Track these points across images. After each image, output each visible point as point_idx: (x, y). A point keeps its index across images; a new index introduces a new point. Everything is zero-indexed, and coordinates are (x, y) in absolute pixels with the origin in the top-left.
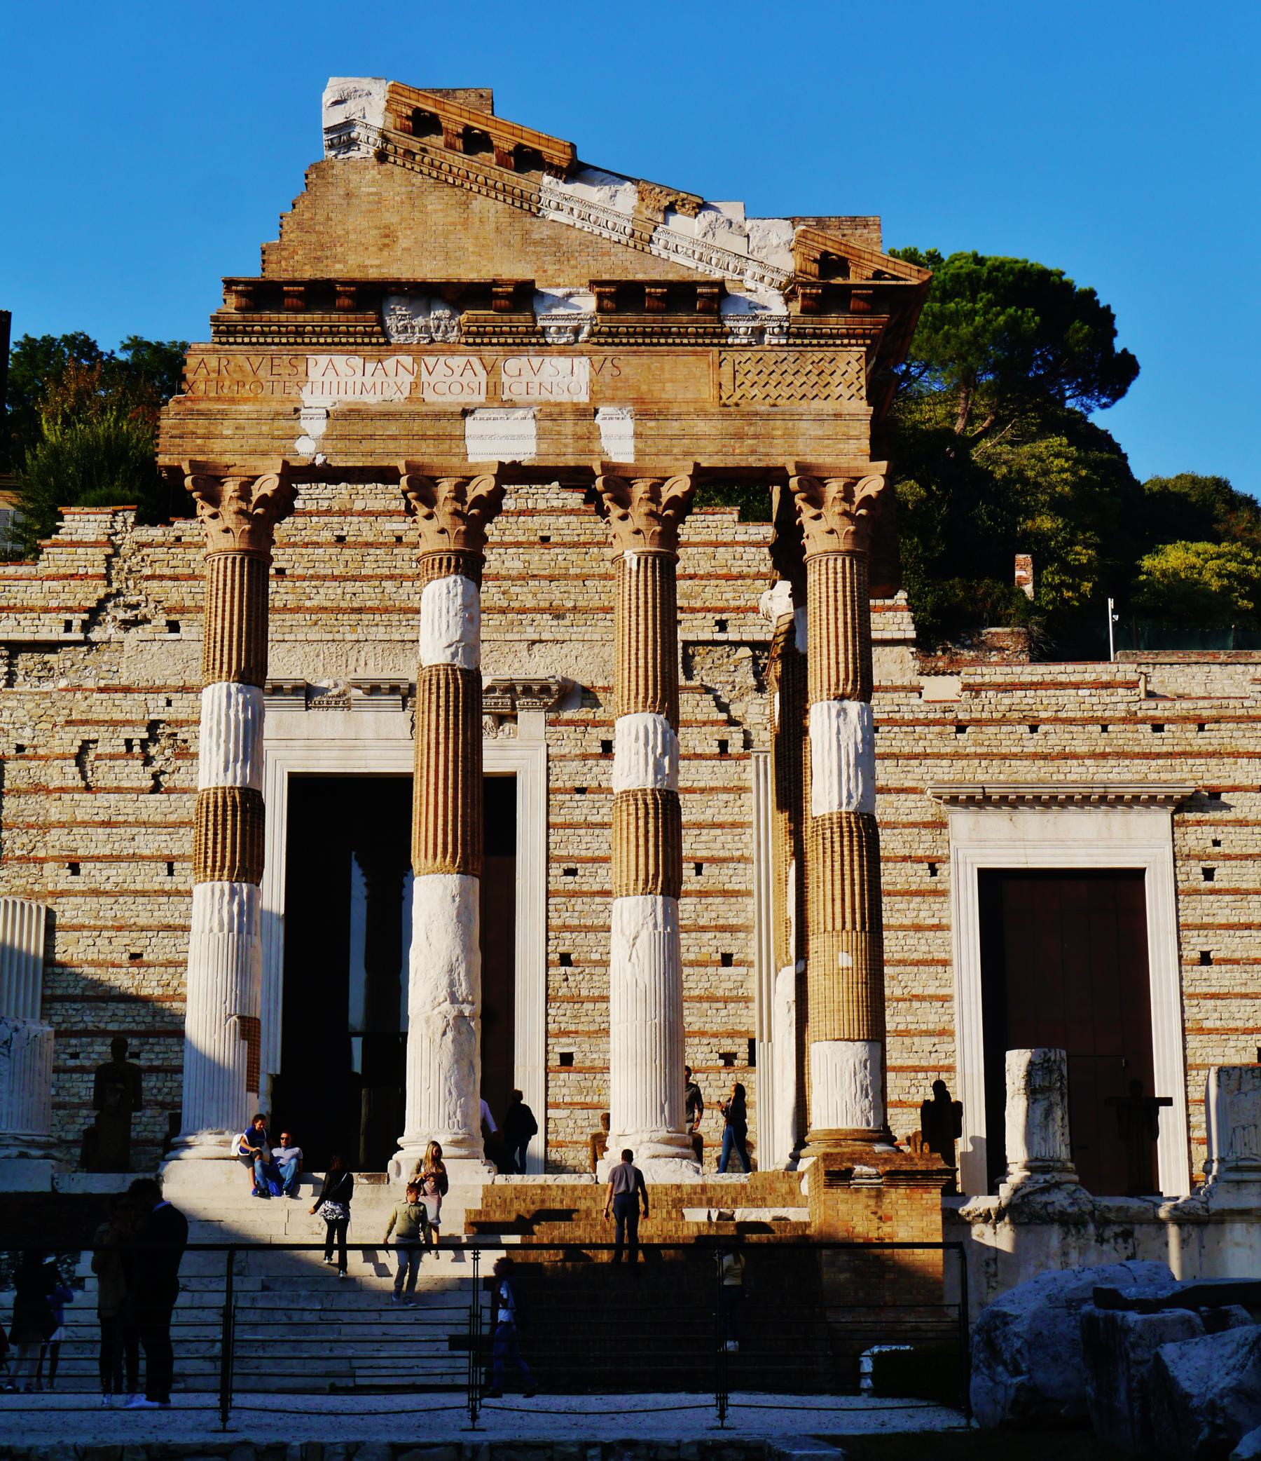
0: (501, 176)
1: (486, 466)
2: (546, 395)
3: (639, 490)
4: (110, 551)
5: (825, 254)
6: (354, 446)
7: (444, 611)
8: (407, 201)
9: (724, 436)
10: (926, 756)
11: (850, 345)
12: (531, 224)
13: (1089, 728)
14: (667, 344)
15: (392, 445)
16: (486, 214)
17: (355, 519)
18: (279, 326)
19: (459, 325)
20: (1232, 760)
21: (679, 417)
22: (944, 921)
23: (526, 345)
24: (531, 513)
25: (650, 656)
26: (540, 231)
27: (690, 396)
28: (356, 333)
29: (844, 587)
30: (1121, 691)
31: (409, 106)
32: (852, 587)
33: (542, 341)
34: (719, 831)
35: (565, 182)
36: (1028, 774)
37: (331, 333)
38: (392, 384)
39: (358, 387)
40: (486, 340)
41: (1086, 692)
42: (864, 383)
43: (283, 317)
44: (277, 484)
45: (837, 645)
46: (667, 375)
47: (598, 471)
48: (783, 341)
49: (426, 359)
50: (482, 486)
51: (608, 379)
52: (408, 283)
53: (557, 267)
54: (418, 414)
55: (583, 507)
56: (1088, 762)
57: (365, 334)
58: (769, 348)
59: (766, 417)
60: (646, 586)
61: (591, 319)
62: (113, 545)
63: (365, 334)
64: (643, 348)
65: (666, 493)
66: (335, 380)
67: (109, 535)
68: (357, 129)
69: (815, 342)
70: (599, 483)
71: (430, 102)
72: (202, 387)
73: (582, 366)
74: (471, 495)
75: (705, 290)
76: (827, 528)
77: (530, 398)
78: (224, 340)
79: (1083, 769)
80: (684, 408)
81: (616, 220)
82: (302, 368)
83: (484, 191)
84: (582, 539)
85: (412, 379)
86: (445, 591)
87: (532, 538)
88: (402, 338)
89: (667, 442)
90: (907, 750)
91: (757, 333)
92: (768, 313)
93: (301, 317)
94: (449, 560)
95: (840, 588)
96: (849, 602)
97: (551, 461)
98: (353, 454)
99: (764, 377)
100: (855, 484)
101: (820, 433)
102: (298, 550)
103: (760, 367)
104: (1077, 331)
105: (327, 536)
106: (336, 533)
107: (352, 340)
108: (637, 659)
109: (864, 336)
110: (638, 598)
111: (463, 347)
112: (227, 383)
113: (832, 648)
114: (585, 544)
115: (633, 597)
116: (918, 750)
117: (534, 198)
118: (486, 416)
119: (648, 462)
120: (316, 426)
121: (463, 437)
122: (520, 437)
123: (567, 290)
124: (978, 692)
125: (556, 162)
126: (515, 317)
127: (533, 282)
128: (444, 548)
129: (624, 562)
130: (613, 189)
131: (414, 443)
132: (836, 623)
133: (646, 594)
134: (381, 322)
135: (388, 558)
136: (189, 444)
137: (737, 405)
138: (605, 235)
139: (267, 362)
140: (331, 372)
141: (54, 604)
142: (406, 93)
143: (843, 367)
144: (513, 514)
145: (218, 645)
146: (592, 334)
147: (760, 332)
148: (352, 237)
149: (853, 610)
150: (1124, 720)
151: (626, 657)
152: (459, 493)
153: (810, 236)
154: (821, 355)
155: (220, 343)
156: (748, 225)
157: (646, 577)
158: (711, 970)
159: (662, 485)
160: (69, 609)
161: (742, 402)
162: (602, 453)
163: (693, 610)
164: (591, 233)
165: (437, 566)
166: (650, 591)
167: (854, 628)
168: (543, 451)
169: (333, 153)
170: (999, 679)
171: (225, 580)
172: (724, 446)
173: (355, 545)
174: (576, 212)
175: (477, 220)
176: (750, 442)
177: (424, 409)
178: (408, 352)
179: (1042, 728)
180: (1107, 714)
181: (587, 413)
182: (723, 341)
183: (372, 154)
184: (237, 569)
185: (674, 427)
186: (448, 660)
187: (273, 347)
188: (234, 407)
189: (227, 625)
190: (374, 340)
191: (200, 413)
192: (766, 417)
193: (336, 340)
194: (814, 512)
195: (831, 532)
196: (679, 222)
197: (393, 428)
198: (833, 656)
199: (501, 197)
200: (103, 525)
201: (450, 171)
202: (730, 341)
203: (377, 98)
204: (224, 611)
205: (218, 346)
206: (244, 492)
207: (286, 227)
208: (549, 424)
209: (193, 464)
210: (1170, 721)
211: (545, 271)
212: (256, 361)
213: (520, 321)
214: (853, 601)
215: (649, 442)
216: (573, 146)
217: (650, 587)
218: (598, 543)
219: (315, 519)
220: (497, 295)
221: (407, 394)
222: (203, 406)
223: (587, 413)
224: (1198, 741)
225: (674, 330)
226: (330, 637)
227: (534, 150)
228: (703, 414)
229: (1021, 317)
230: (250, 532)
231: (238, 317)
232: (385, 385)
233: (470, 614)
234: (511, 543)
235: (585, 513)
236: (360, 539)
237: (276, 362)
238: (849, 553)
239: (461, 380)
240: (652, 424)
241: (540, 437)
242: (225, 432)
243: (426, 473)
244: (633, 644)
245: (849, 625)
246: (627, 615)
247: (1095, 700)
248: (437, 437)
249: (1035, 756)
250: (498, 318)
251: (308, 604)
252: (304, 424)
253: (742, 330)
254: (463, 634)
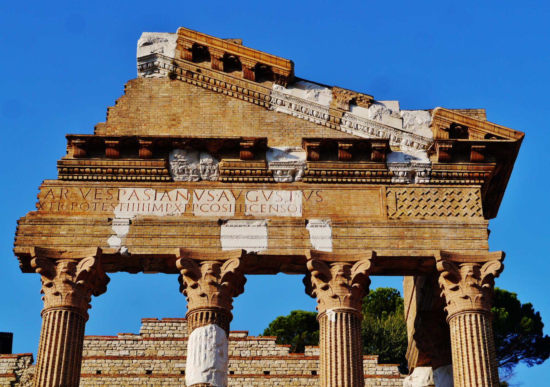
0: (246, 85)
1: (235, 253)
2: (274, 212)
3: (336, 270)
4: (13, 379)
5: (453, 125)
6: (147, 242)
7: (203, 347)
8: (188, 101)
9: (390, 238)
11: (470, 184)
12: (265, 114)
14: (352, 182)
15: (171, 242)
16: (237, 109)
17: (158, 361)
18: (102, 169)
19: (218, 168)
21: (361, 225)
23: (261, 182)
24: (259, 358)
25: (345, 378)
26: (270, 118)
27: (368, 213)
28: (151, 173)
29: (478, 333)
31: (190, 42)
32: (483, 334)
33: (271, 179)
35: (287, 88)
37: (135, 173)
38: (174, 205)
40: (235, 179)
42: (481, 207)
43: (104, 162)
44: (93, 263)
45: (476, 372)
46: (352, 201)
47: (309, 257)
48: (427, 181)
49: (196, 190)
50: (231, 266)
51: (314, 203)
52: (185, 139)
53: (281, 138)
54: (190, 222)
55: (288, 355)
57: (157, 174)
58: (418, 185)
59: (419, 226)
60: (342, 332)
61: (303, 165)
62: (16, 375)
63: (157, 174)
64: (337, 185)
65: (354, 272)
66: (136, 202)
67: (14, 370)
68: (158, 60)
69: (448, 181)
70: (309, 265)
71: (203, 39)
72: (49, 206)
73: (297, 196)
74: (224, 271)
75: (377, 145)
76: (463, 296)
77: (263, 214)
78: (65, 177)
80: (364, 220)
81: (319, 110)
82: (115, 196)
83: (236, 95)
84: (288, 373)
85: (186, 202)
86: (204, 334)
87: (259, 372)
88: (181, 177)
89: (353, 241)
91: (410, 175)
92: (417, 162)
93: (116, 163)
94: (207, 314)
95: (475, 334)
96: (482, 344)
97: (277, 252)
98: (146, 247)
99: (415, 203)
100: (480, 267)
101: (454, 236)
102: (124, 379)
103: (413, 196)
104: (525, 322)
105: (141, 370)
106: (147, 369)
107: (148, 178)
108: (337, 380)
109: (479, 178)
110: (336, 340)
111: (220, 183)
112: (65, 204)
113: (473, 374)
114: (290, 375)
115: (333, 340)
117: (267, 98)
118: (234, 224)
121: (219, 237)
122: (256, 237)
123: (287, 147)
125: (281, 73)
126: (254, 164)
127: (265, 140)
128: (204, 305)
129: (326, 318)
130: (317, 92)
131: (187, 240)
132: (474, 357)
133: (342, 337)
134: (168, 166)
135: (176, 383)
137: (399, 218)
138: (312, 120)
139: (93, 191)
140: (134, 199)
142: (189, 34)
143: (467, 197)
144: (248, 359)
145: (44, 370)
146: (303, 176)
147: (412, 175)
148: (152, 120)
149: (485, 349)
151: (329, 380)
152: (216, 270)
153: (443, 113)
154: (452, 190)
155: (63, 179)
156: (402, 113)
157: (341, 326)
159: (351, 267)
161: (402, 217)
164: (303, 119)
165: (199, 317)
166: (344, 335)
167: (486, 361)
168: (272, 246)
169: (143, 74)
171: (53, 327)
172: (391, 244)
173: (157, 376)
174: (293, 106)
175: (231, 111)
176: (408, 241)
177: (193, 219)
178: (185, 187)
181: (301, 223)
182: (388, 181)
183: (167, 74)
184: (62, 319)
185: (359, 232)
186: (205, 380)
187: (97, 183)
188: (69, 218)
189: (51, 356)
190: (163, 178)
191: (46, 221)
192: (419, 226)
193: (139, 178)
194: (453, 285)
195: (466, 297)
196: (357, 110)
197: (173, 231)
198: (473, 379)
199: (246, 99)
200: (11, 364)
201: (215, 84)
202: (393, 180)
203: (171, 43)
204: (50, 347)
205: (61, 182)
206: (71, 269)
207: (110, 114)
208: (276, 229)
209: (37, 250)
211: (274, 140)
213: (257, 165)
214: (484, 343)
215: (342, 240)
216: (292, 63)
217: (344, 333)
218: (297, 375)
219: (135, 361)
220: (243, 148)
221: (183, 211)
225: (357, 173)
227: (269, 67)
228: (377, 224)
229: (499, 312)
230: (73, 294)
231: (75, 162)
232: (169, 206)
233: (221, 350)
234: (247, 375)
235: (290, 358)
236: (160, 372)
237: (99, 191)
238: (479, 311)
239: (219, 203)
240: (344, 230)
241: (269, 237)
242: (61, 233)
243: (193, 257)
244: (334, 370)
245: (483, 359)
246: (328, 351)
248: (202, 237)
250: (243, 164)
252: (115, 229)
253: (401, 174)
254: (215, 363)
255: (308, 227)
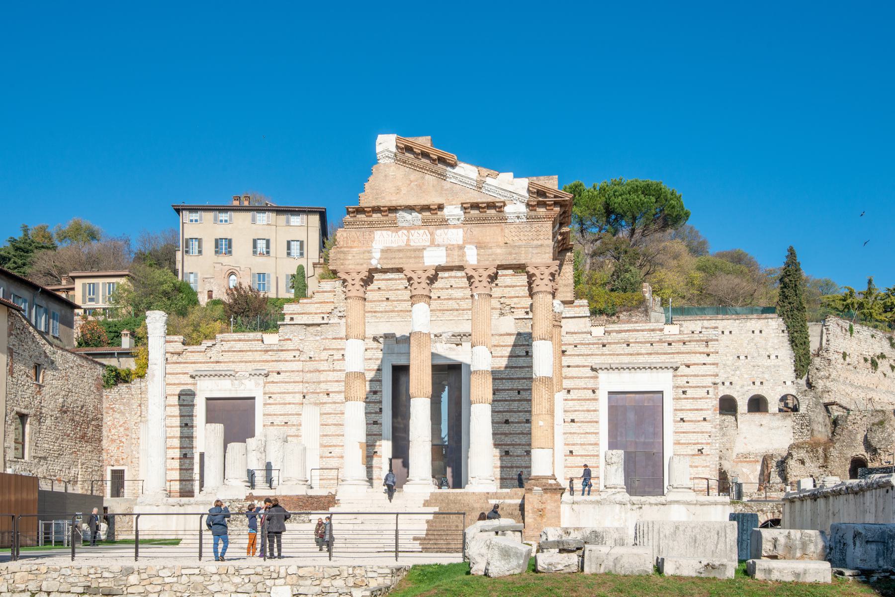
6: (389, 261)
10: (592, 355)
13: (647, 345)
15: (401, 261)
20: (694, 355)
21: (491, 248)
22: (597, 409)
30: (658, 332)
34: (525, 381)
36: (626, 359)
39: (390, 241)
41: (646, 333)
56: (645, 356)
73: (460, 231)
79: (644, 359)
82: (373, 236)
85: (407, 238)
90: (586, 353)
112: (349, 242)
116: (589, 353)
119: (482, 263)
120: (377, 255)
121: (423, 257)
124: (610, 333)
136: (338, 262)
139: (362, 234)
141: (318, 311)
150: (658, 342)
158: (522, 425)
160: (323, 313)
162: (467, 261)
163: (518, 308)
170: (617, 329)
179: (631, 345)
180: (653, 340)
181: (461, 248)
192: (519, 247)
197: (401, 255)
208: (450, 252)
210: (673, 342)
212: (358, 234)
221: (405, 243)
222: (342, 249)
223: (461, 248)
224: (683, 348)
226: (403, 320)
228: (498, 246)
240: (483, 251)
241: (448, 256)
247: (649, 335)
248: (415, 257)
249: (628, 354)
251: (396, 309)
252: (373, 254)
255: (466, 250)
